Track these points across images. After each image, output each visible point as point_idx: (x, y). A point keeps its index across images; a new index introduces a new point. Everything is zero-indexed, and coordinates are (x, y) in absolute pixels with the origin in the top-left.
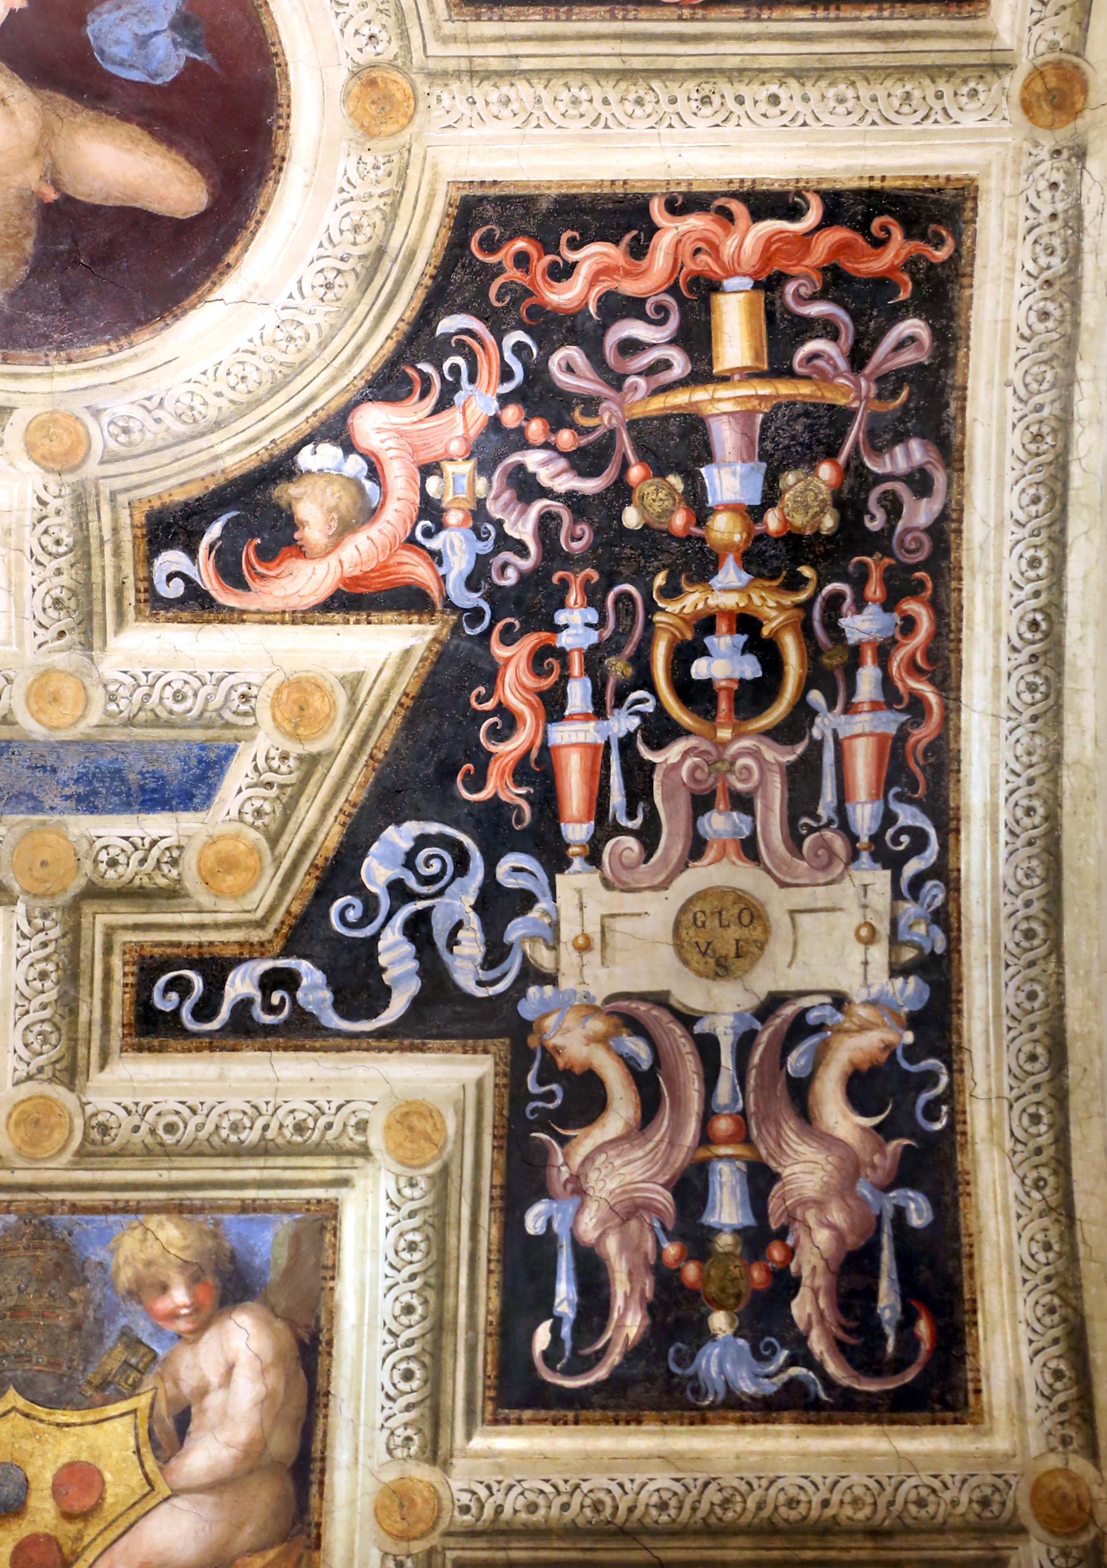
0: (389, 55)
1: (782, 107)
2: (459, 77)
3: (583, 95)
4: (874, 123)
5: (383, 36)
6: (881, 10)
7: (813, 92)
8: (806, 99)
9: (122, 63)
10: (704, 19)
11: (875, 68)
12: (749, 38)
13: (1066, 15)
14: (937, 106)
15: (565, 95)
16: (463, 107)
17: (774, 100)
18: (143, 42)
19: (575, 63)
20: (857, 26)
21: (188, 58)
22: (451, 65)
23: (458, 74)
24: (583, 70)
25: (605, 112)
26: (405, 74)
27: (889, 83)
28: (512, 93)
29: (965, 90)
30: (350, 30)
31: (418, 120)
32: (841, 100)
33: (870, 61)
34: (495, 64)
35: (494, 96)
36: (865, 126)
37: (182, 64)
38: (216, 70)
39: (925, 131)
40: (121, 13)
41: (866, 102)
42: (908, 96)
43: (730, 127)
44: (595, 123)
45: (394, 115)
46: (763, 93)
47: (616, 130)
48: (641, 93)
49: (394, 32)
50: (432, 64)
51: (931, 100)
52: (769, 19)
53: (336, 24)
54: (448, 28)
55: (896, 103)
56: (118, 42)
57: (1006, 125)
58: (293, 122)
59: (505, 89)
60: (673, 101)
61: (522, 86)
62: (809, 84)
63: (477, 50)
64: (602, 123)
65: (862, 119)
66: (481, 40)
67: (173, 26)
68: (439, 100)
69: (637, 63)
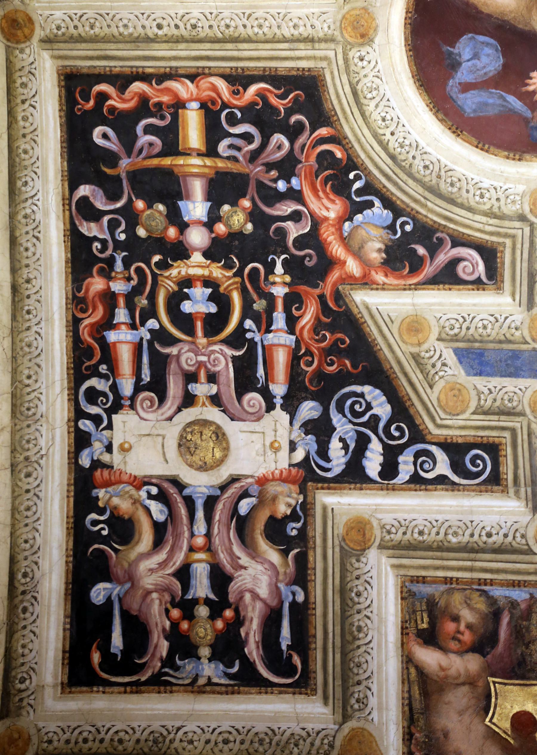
0: (354, 50)
1: (155, 23)
2: (319, 39)
3: (256, 30)
4: (108, 14)
5: (356, 60)
6: (111, 71)
7: (140, 30)
8: (144, 27)
9: (488, 44)
10: (198, 68)
11: (110, 42)
12: (175, 58)
13: (18, 66)
14: (76, 22)
15: (266, 30)
16: (317, 24)
17: (159, 27)
18: (476, 56)
19: (261, 46)
20: (121, 63)
21: (454, 47)
22: (323, 45)
23: (320, 40)
24: (257, 42)
25: (245, 21)
26: (347, 41)
27: (102, 34)
28: (292, 31)
29: (63, 30)
30: (373, 63)
31: (340, 17)
32: (125, 26)
33: (113, 46)
34: (301, 46)
35: (301, 29)
36: (112, 13)
37: (458, 45)
38: (440, 42)
39: (81, 9)
40: (485, 71)
41: (113, 25)
42: (92, 27)
43: (181, 12)
44: (250, 15)
45: (352, 19)
46: (165, 30)
47: (239, 12)
48: (227, 31)
49: (351, 62)
50: (332, 46)
51: (80, 25)
52: (165, 68)
53: (380, 66)
54: (324, 64)
55: (97, 24)
56: (488, 55)
57: (40, 12)
58: (404, 15)
59: (296, 33)
60: (211, 27)
61: (287, 34)
62: (143, 35)
63: (310, 53)
64: (246, 15)
65: (114, 16)
66: (308, 58)
67: (459, 64)
68: (329, 27)
69: (229, 46)
